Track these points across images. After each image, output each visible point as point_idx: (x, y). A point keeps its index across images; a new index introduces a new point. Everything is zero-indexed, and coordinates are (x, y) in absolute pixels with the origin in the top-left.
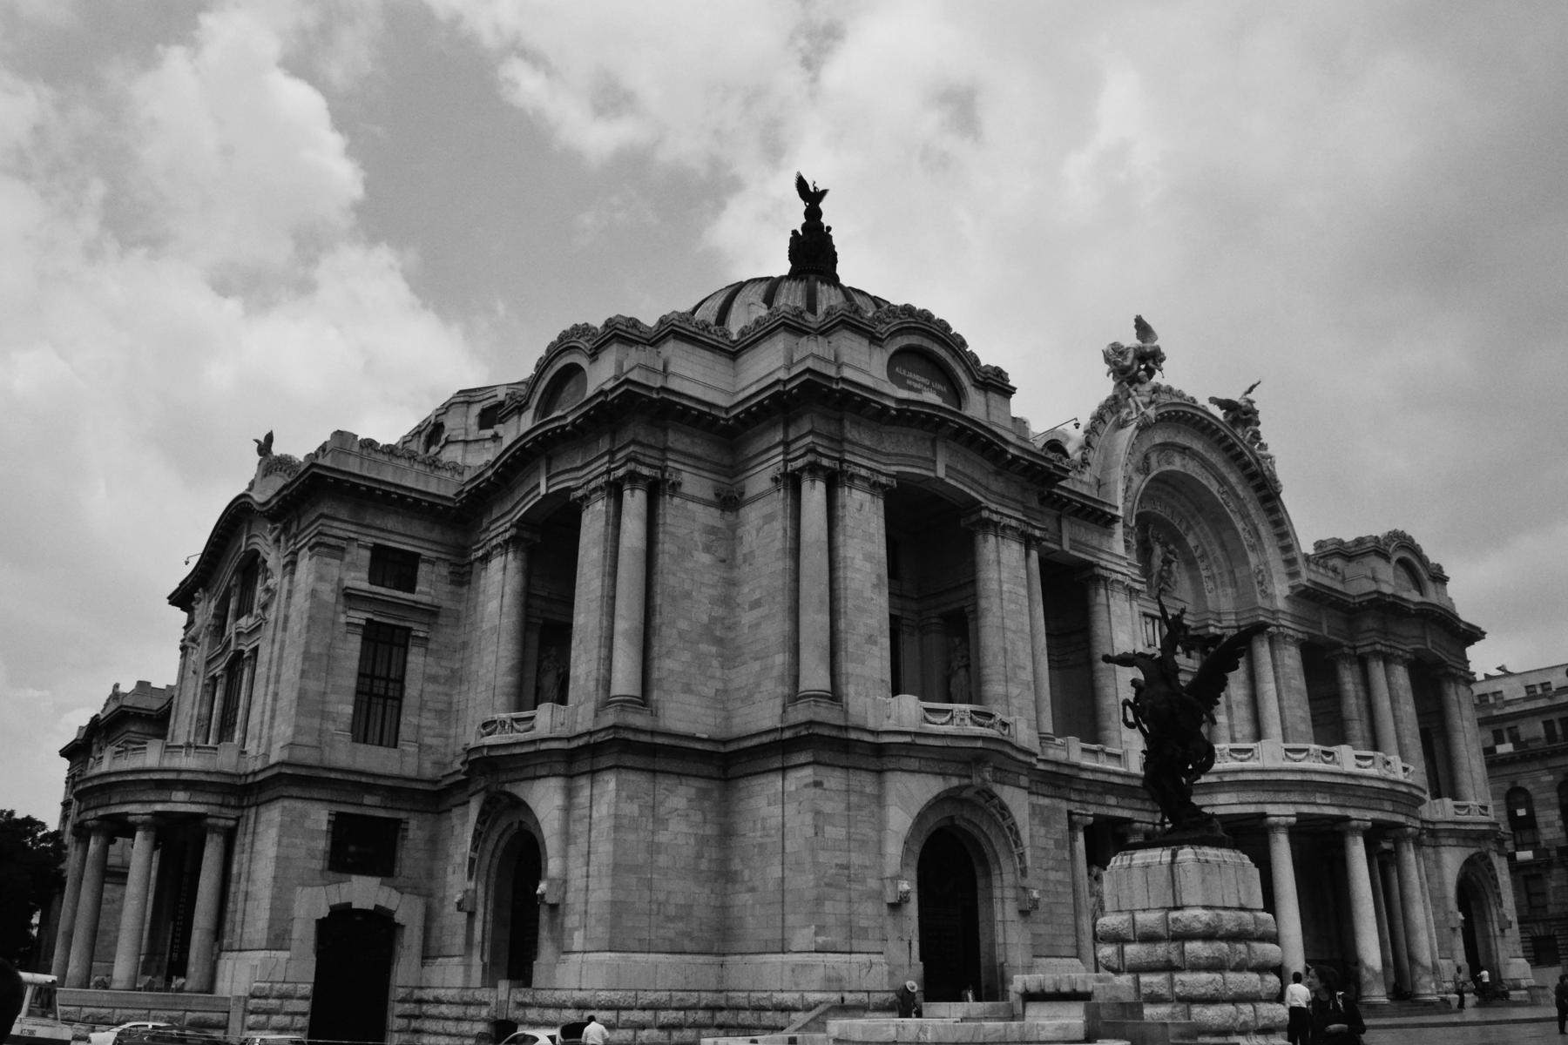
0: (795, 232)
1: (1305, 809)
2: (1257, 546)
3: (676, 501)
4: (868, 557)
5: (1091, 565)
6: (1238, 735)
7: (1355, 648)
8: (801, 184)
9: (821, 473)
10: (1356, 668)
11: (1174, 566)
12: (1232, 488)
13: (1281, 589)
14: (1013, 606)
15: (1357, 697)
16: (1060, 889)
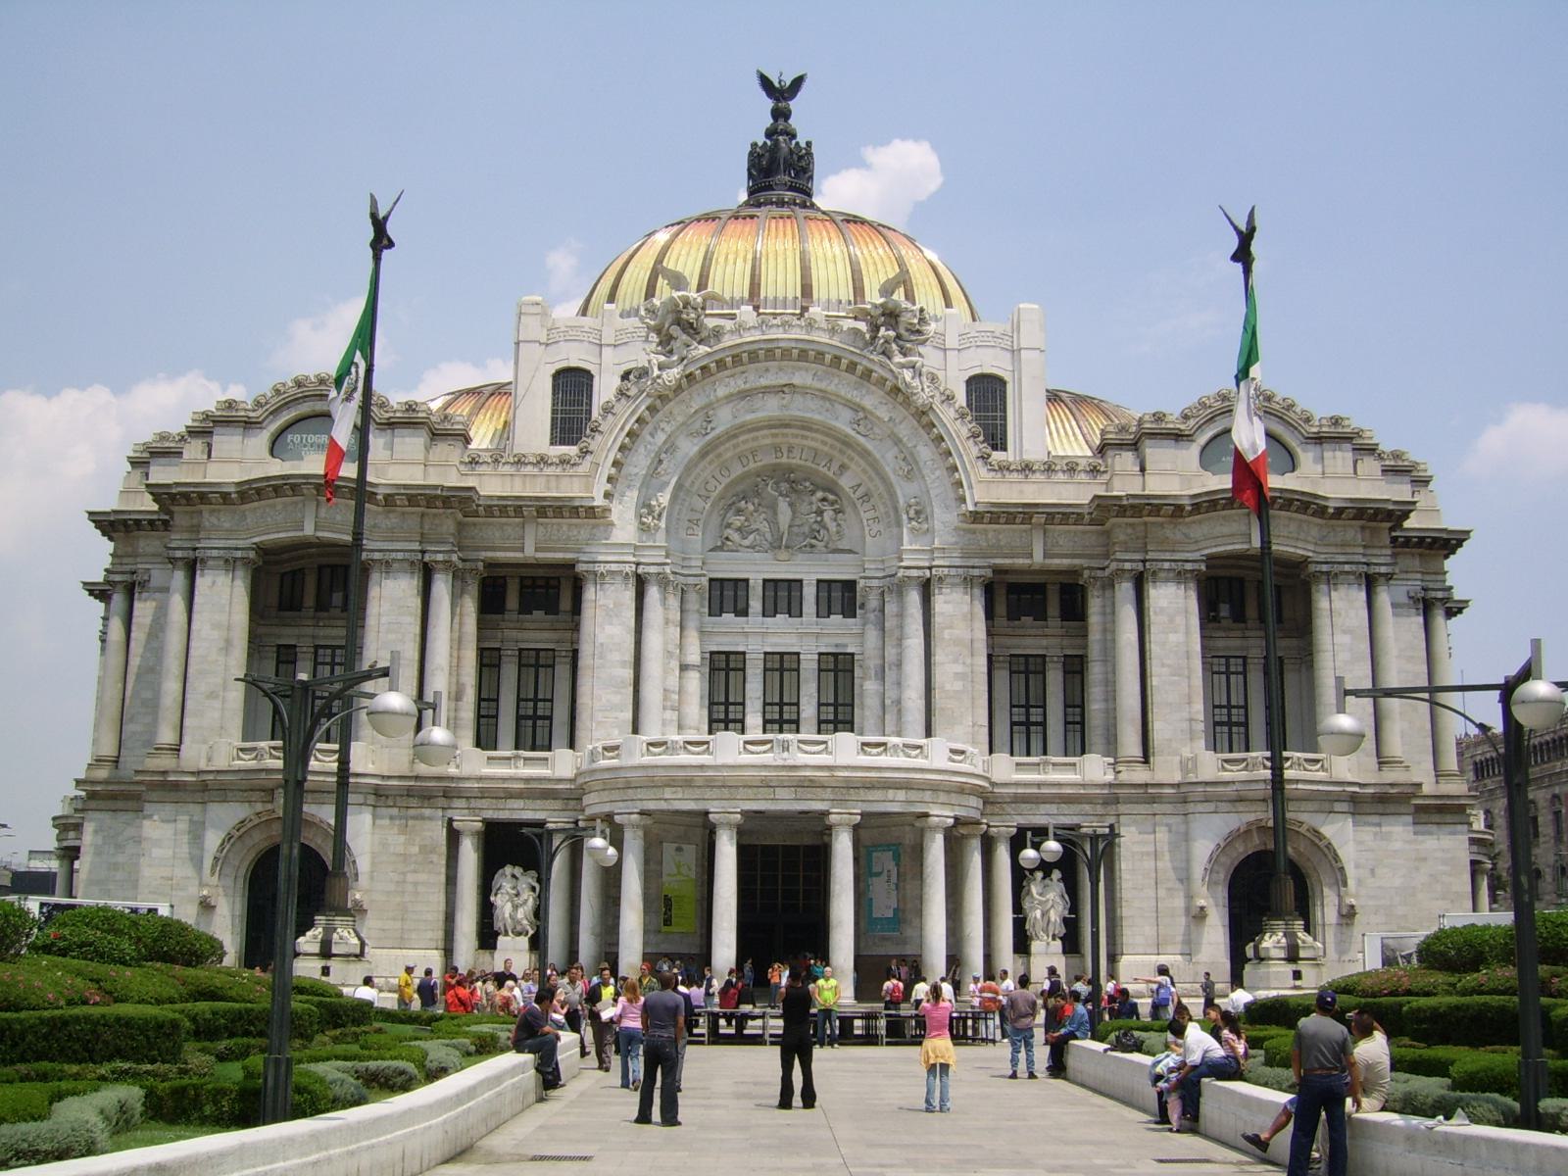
0: (754, 145)
1: (651, 806)
2: (912, 471)
3: (145, 595)
4: (216, 626)
5: (570, 566)
6: (888, 702)
7: (1103, 569)
8: (765, 83)
9: (180, 563)
10: (1108, 593)
11: (828, 515)
12: (872, 413)
13: (944, 520)
14: (391, 637)
15: (1105, 631)
16: (420, 889)
